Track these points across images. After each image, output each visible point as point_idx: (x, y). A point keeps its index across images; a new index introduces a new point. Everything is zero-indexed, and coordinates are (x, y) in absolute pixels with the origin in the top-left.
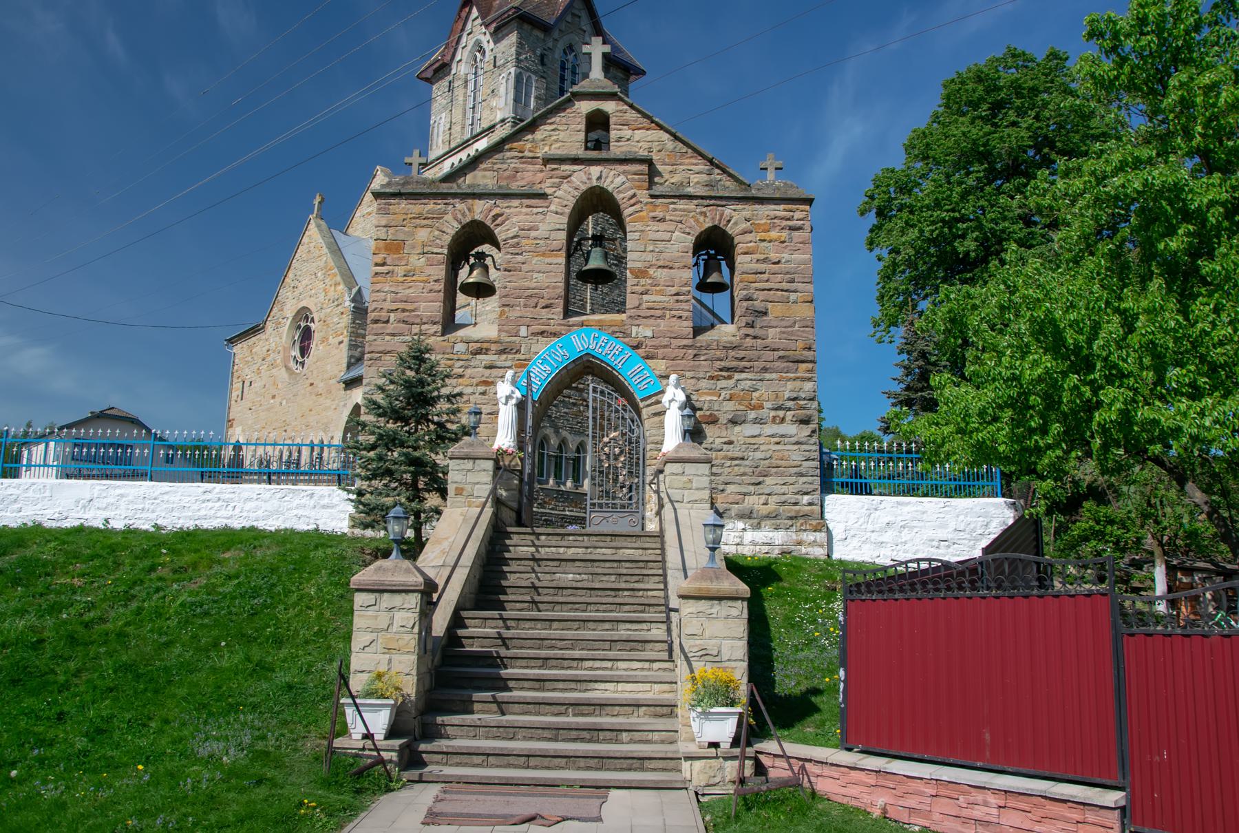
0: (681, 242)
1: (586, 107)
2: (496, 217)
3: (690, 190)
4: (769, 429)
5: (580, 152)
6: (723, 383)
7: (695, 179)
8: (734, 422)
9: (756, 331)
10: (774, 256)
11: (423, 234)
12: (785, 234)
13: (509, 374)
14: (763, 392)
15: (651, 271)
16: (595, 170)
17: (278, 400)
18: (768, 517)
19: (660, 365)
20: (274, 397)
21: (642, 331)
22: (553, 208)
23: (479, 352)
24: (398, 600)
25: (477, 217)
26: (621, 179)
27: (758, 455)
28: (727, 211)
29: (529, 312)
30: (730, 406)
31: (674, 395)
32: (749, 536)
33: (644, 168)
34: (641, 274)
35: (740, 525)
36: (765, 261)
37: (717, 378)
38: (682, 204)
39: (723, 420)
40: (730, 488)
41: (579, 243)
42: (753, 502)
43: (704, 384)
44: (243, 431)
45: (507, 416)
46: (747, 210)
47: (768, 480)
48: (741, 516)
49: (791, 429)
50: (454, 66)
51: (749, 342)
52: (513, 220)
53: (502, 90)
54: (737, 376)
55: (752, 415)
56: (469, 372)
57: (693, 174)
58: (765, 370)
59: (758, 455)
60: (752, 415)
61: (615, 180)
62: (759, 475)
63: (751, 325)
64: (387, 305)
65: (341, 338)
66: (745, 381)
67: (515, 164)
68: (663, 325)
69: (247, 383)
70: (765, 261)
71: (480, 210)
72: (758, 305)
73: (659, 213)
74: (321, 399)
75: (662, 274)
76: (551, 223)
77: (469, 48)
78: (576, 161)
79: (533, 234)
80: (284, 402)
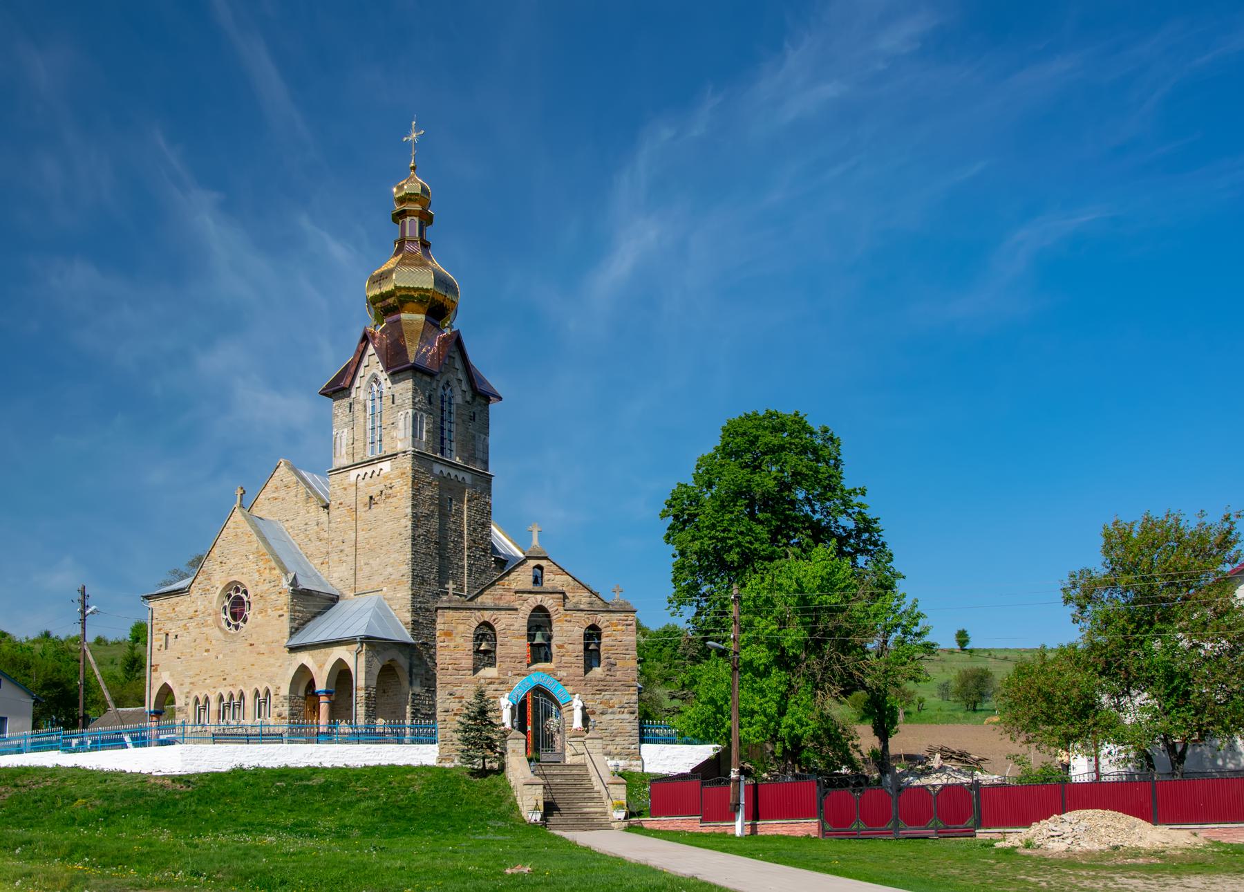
0: (578, 632)
3: (582, 607)
4: (617, 716)
5: (530, 587)
7: (584, 600)
8: (602, 714)
10: (619, 638)
11: (461, 628)
13: (507, 695)
14: (615, 700)
16: (539, 597)
17: (212, 654)
19: (570, 689)
20: (207, 651)
21: (562, 673)
29: (512, 665)
30: (601, 707)
31: (577, 703)
38: (579, 614)
44: (172, 675)
46: (607, 616)
49: (626, 716)
50: (353, 390)
52: (502, 622)
53: (401, 424)
57: (582, 598)
61: (549, 602)
62: (614, 736)
64: (447, 661)
65: (281, 612)
66: (607, 695)
67: (501, 592)
69: (171, 638)
71: (487, 616)
72: (612, 661)
74: (262, 657)
75: (570, 647)
76: (520, 622)
77: (367, 378)
78: (530, 592)
80: (221, 656)
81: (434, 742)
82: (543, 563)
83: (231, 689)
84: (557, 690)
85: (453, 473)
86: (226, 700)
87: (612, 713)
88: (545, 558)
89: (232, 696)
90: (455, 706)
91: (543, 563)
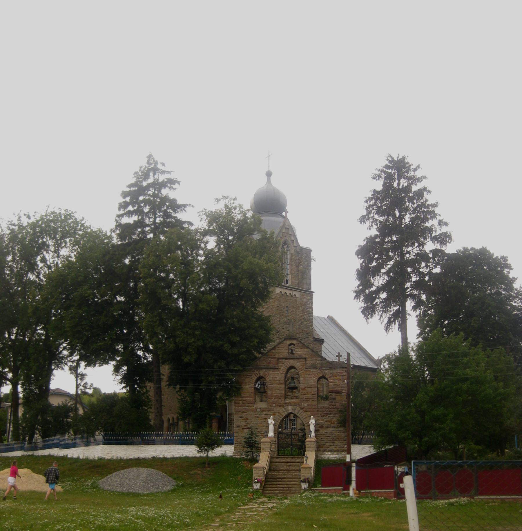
1: (289, 342)
2: (266, 375)
6: (325, 417)
8: (328, 427)
9: (334, 404)
12: (341, 377)
15: (306, 389)
16: (292, 361)
18: (336, 451)
19: (309, 413)
22: (281, 372)
23: (264, 411)
24: (260, 469)
25: (261, 375)
26: (298, 363)
27: (334, 435)
28: (326, 371)
30: (326, 423)
31: (313, 421)
32: (332, 456)
33: (304, 360)
34: (304, 389)
35: (329, 453)
36: (336, 385)
37: (323, 416)
39: (325, 427)
40: (327, 444)
41: (288, 380)
42: (332, 447)
43: (320, 418)
45: (271, 428)
47: (336, 442)
48: (329, 451)
51: (331, 406)
54: (329, 415)
55: (332, 425)
56: (261, 416)
58: (335, 414)
59: (334, 435)
60: (332, 425)
61: (297, 364)
63: (331, 402)
68: (309, 403)
70: (336, 385)
71: (262, 373)
73: (308, 373)
78: (286, 359)
79: (276, 379)
80: (169, 398)
81: (232, 444)
82: (295, 342)
83: (173, 415)
84: (302, 414)
85: (288, 292)
86: (171, 421)
87: (333, 427)
88: (295, 339)
89: (173, 419)
90: (243, 424)
91: (295, 342)
